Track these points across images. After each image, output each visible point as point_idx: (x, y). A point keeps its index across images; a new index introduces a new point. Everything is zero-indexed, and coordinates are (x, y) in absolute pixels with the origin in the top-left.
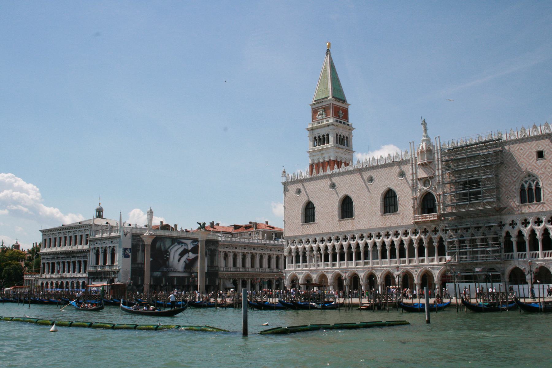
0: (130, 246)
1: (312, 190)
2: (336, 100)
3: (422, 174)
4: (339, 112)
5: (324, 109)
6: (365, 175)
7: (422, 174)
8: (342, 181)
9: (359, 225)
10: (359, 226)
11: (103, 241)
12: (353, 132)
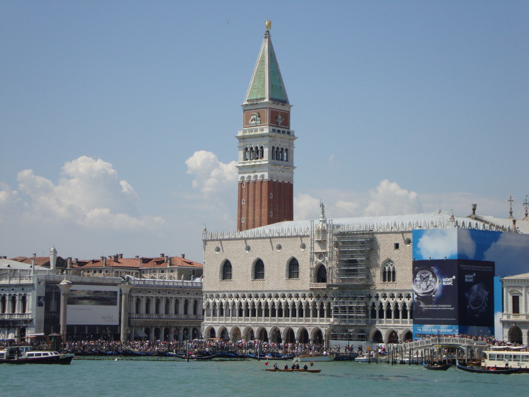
0: (44, 295)
1: (230, 250)
2: (274, 103)
3: (318, 249)
4: (277, 118)
5: (259, 113)
6: (275, 243)
7: (318, 249)
8: (256, 245)
9: (269, 286)
10: (268, 287)
11: (12, 288)
12: (295, 142)
